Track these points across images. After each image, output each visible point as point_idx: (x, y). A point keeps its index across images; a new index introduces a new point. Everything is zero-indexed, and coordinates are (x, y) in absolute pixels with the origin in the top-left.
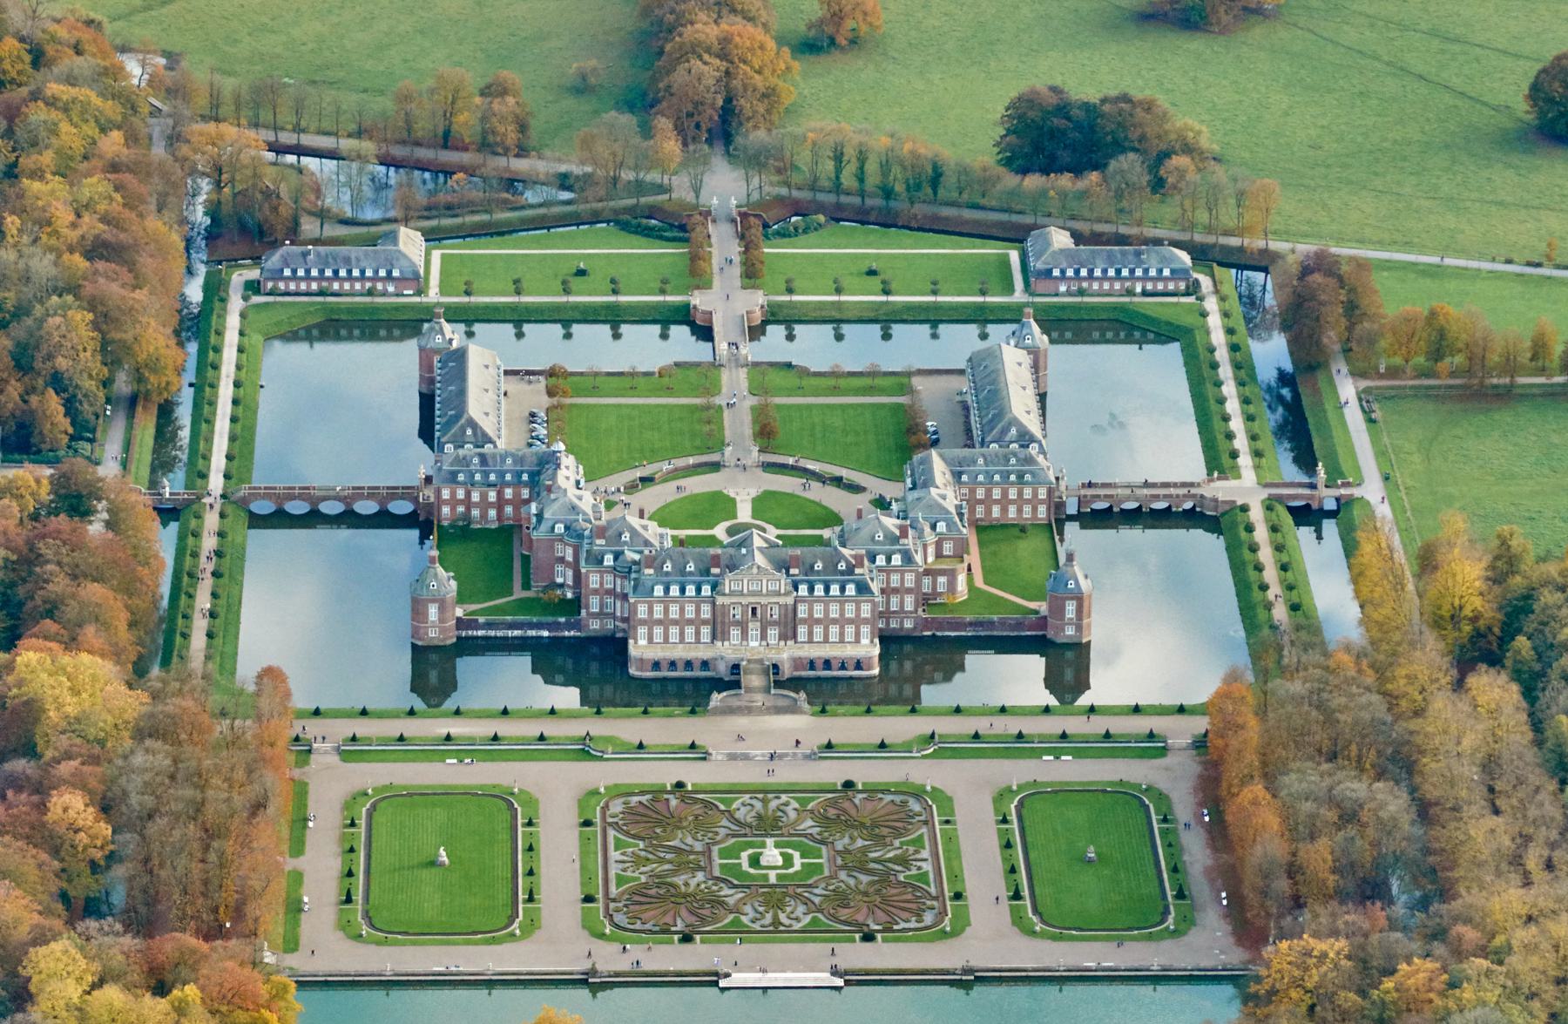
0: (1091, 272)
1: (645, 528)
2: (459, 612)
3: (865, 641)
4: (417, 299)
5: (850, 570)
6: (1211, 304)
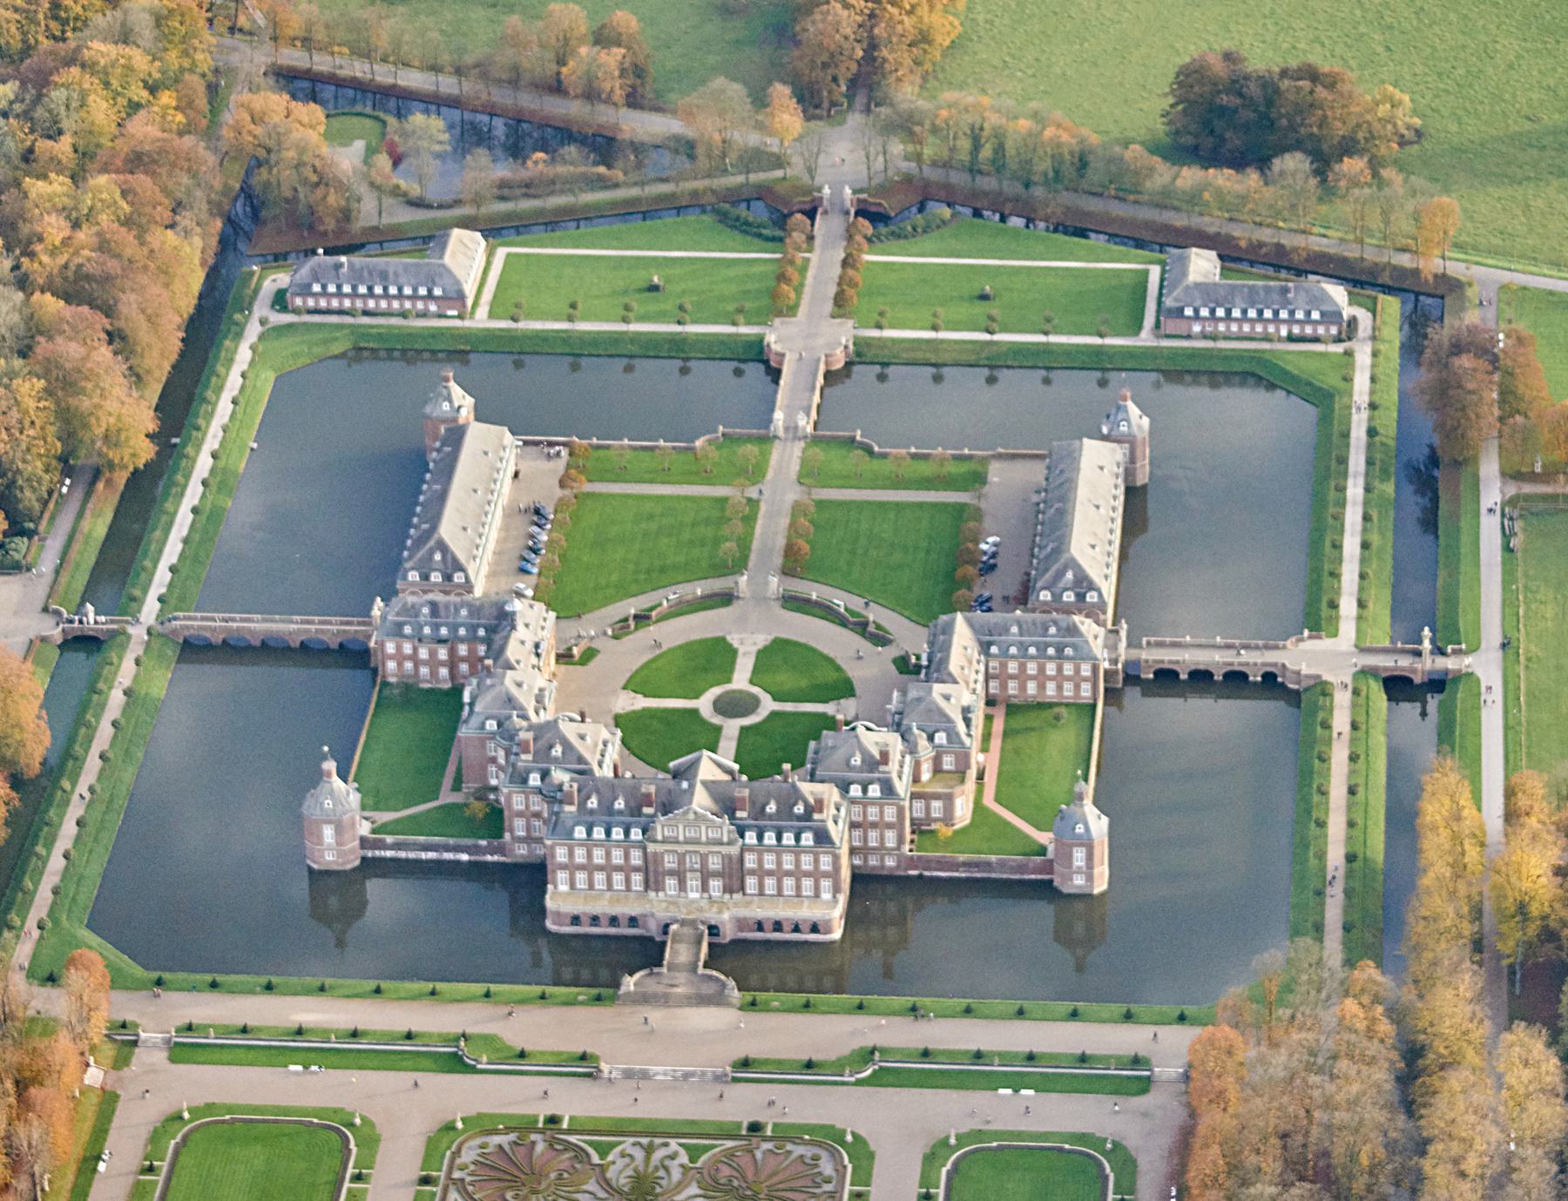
0: (1228, 312)
1: (582, 737)
2: (364, 829)
3: (826, 896)
4: (458, 323)
5: (807, 816)
6: (1363, 357)
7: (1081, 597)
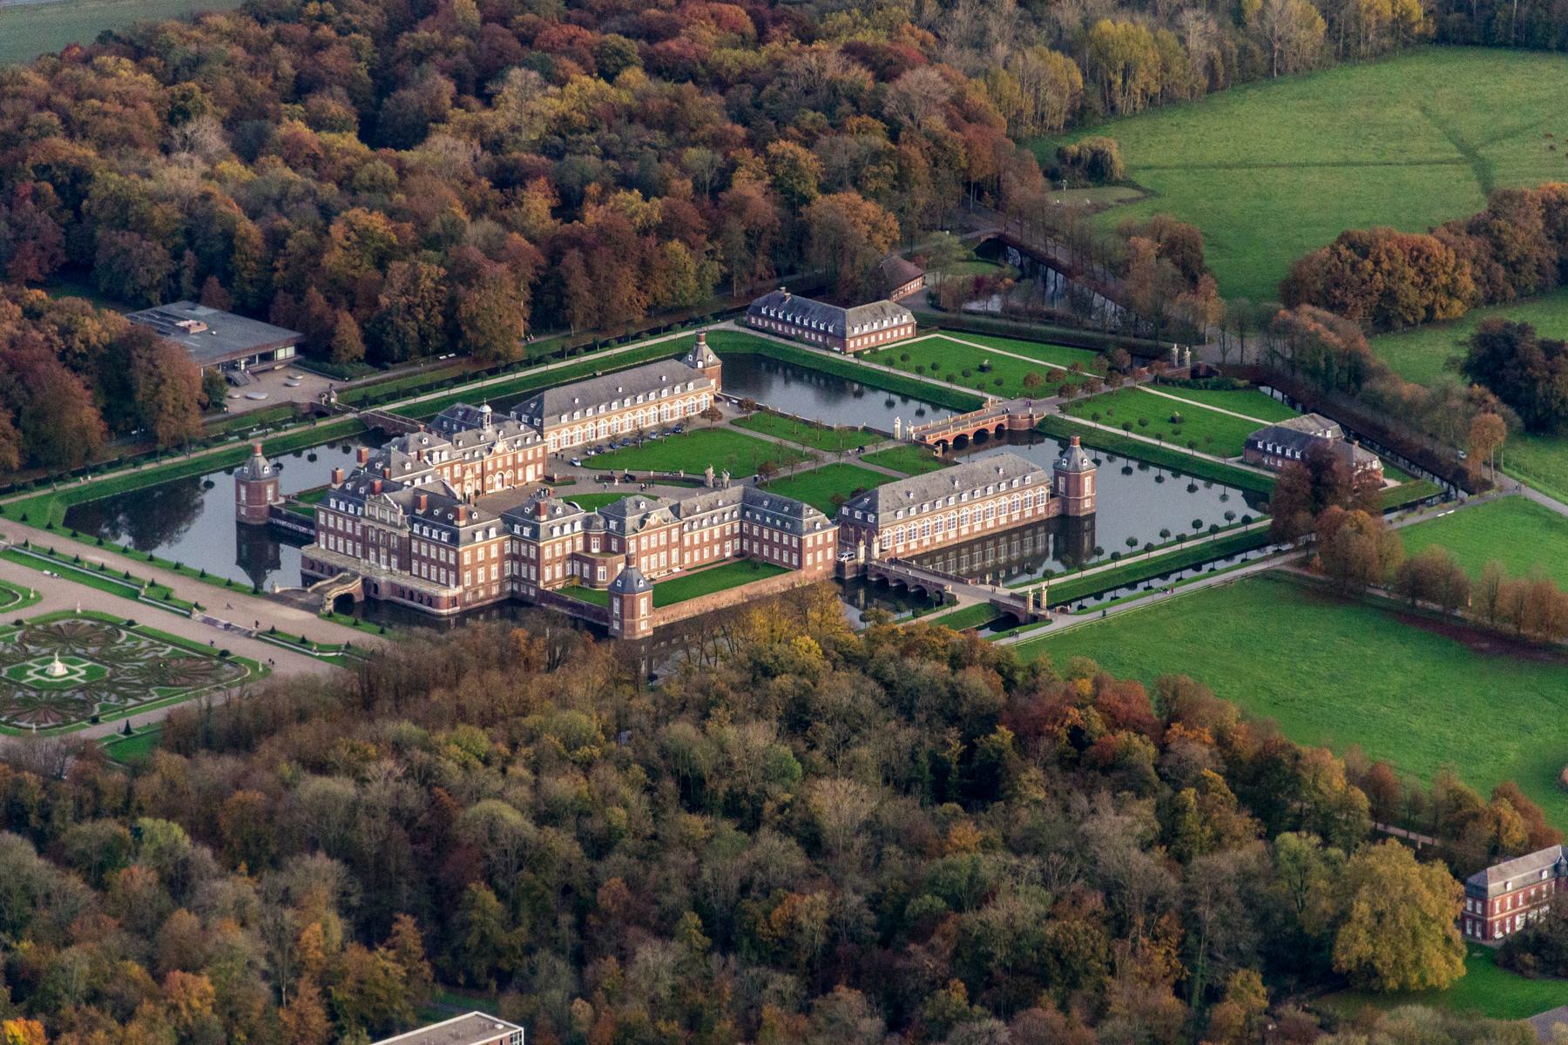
0: (1284, 451)
5: (451, 522)
7: (865, 516)
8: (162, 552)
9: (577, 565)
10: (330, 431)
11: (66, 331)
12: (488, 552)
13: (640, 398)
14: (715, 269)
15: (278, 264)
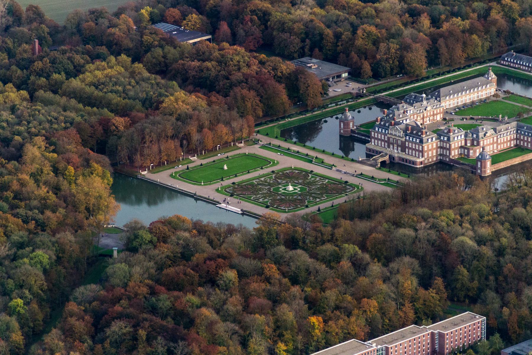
5: (420, 136)
8: (308, 144)
9: (463, 150)
10: (364, 102)
11: (275, 69)
12: (432, 146)
13: (472, 90)
14: (487, 44)
15: (339, 44)
